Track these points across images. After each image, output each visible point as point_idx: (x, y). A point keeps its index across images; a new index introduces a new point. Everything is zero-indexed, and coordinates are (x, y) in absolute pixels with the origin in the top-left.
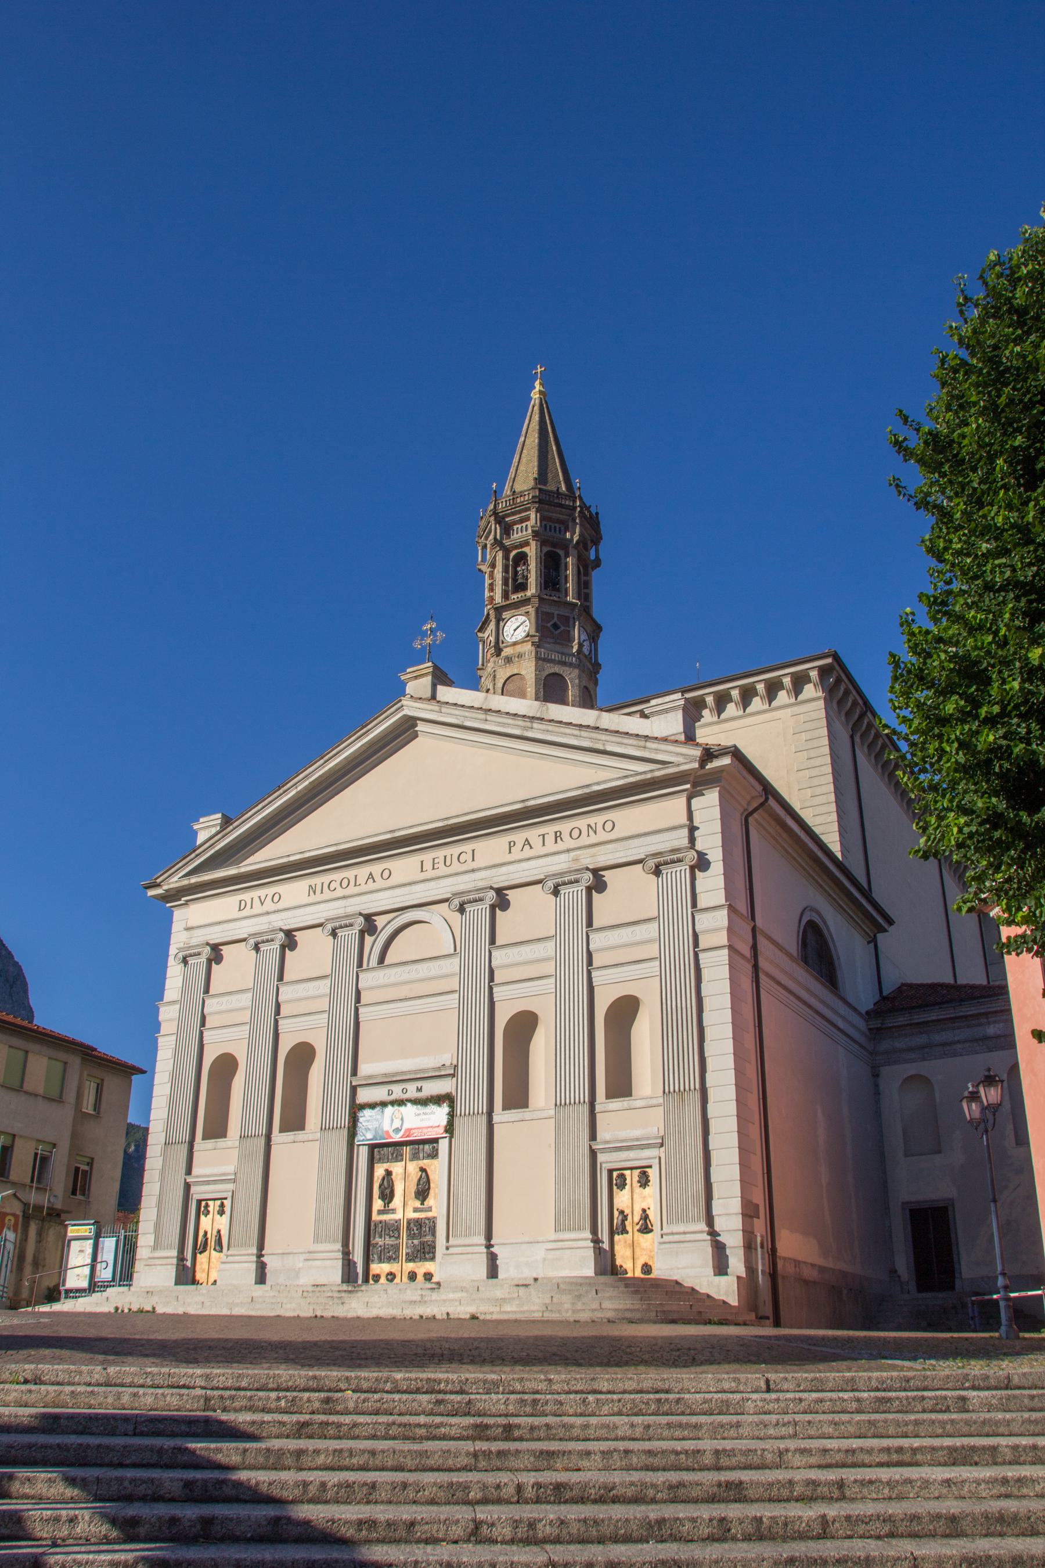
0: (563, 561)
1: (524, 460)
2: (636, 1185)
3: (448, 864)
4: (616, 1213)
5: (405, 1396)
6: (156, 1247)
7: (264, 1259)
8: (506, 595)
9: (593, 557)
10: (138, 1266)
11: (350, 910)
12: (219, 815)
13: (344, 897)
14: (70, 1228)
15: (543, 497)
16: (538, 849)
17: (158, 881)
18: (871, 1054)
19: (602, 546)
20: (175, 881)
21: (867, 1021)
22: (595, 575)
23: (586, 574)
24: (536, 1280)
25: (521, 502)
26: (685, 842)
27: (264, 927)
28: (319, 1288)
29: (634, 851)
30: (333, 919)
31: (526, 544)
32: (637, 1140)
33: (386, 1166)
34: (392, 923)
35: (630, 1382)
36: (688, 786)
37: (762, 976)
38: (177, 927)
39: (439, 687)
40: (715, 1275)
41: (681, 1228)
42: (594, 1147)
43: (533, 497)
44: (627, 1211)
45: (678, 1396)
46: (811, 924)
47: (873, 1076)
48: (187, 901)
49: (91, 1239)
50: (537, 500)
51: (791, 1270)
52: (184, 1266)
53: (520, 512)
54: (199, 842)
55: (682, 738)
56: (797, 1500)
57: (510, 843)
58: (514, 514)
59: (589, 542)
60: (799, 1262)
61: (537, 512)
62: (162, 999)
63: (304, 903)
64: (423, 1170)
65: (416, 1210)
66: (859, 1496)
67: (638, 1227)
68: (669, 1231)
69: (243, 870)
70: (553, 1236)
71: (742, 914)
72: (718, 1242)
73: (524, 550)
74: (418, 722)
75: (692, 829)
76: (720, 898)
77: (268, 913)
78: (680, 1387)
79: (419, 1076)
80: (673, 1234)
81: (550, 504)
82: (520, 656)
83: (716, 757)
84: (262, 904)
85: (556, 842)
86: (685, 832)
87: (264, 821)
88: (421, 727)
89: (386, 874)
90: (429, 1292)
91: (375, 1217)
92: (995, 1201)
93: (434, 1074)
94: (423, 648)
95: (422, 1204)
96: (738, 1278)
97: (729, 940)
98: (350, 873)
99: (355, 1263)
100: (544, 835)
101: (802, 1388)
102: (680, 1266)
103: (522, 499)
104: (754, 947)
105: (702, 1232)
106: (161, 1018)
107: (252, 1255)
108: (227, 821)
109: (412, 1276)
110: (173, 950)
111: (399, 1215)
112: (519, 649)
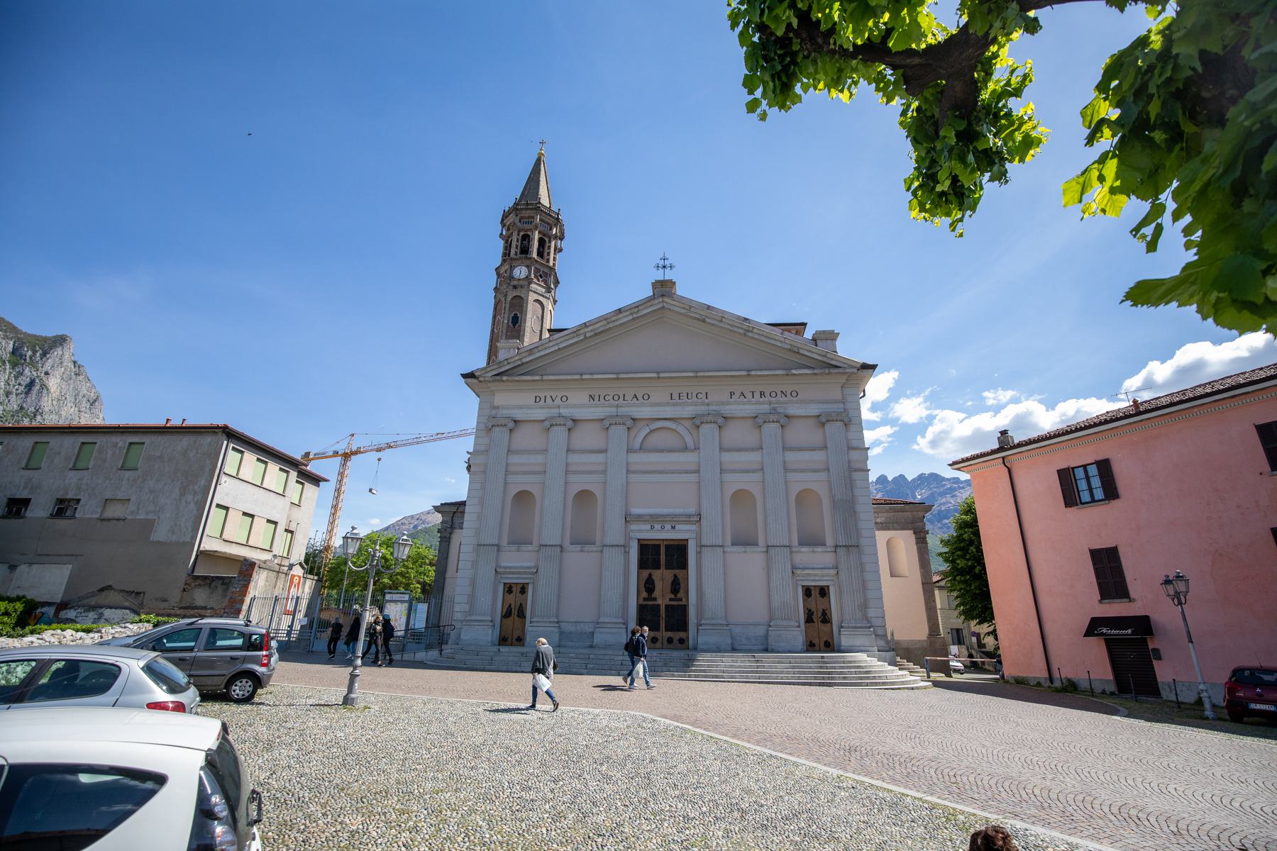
0: (547, 244)
2: (818, 596)
8: (516, 254)
33: (649, 571)
57: (731, 393)
64: (675, 576)
65: (671, 600)
67: (820, 620)
82: (522, 287)
92: (1191, 641)
95: (675, 596)
109: (670, 640)
112: (521, 283)
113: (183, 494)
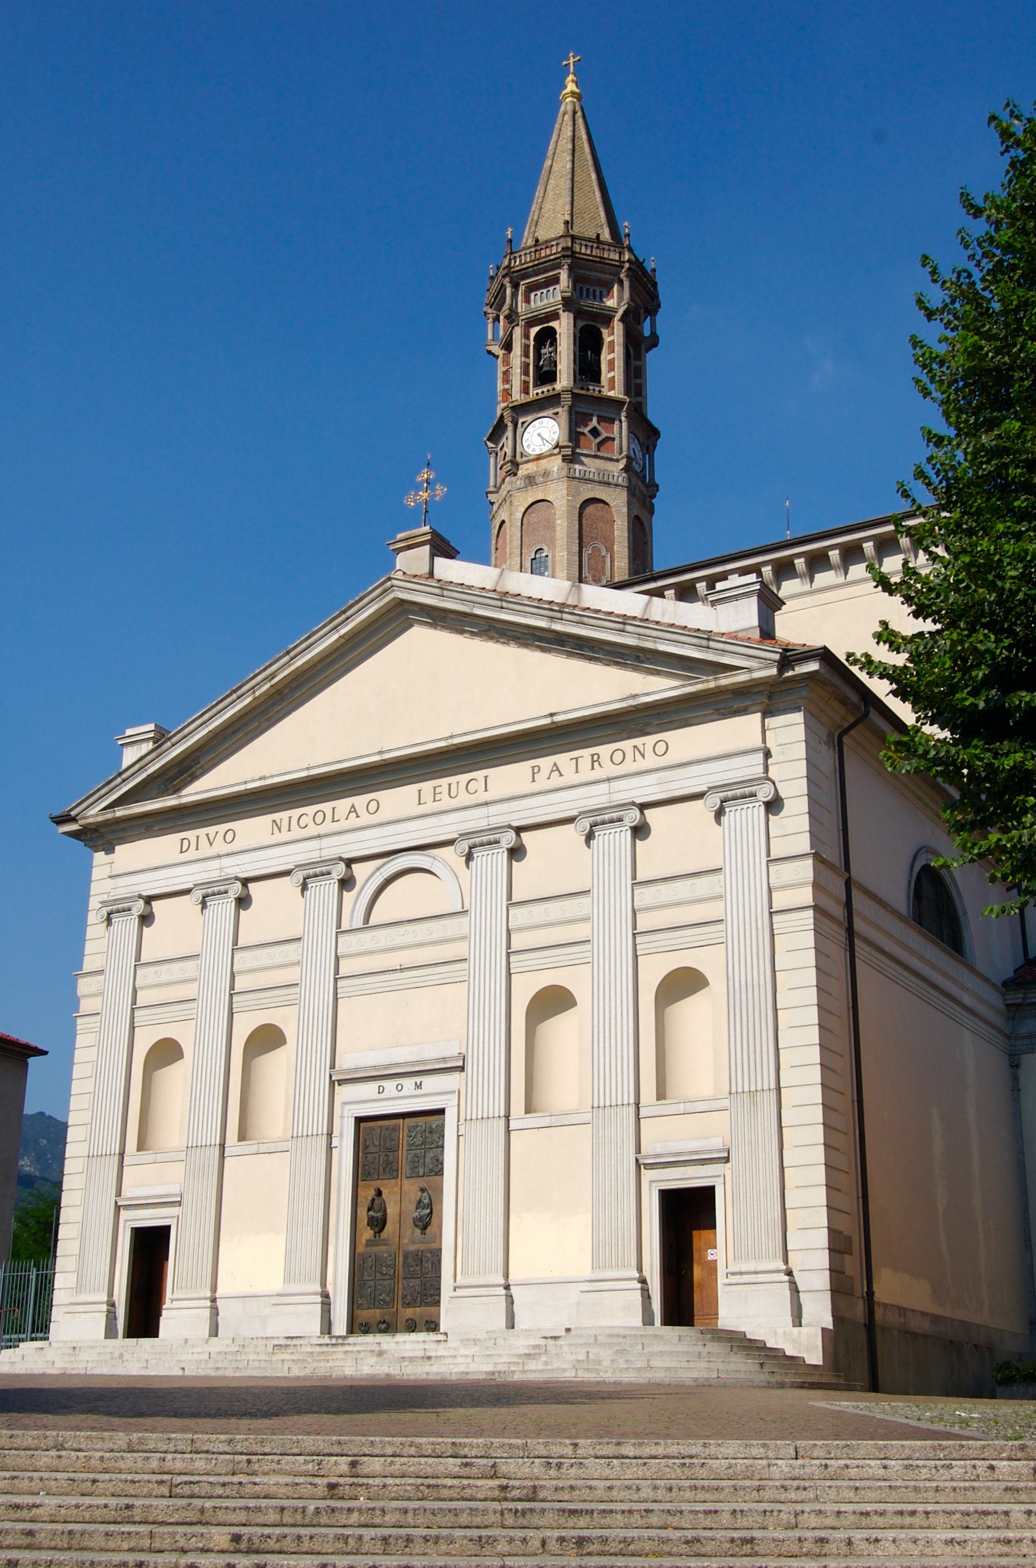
1: (550, 194)
3: (453, 793)
5: (431, 1460)
6: (79, 1288)
8: (526, 390)
9: (647, 333)
10: (56, 1314)
11: (327, 854)
12: (151, 727)
13: (319, 837)
17: (73, 813)
18: (1009, 1038)
19: (659, 318)
21: (1004, 995)
22: (652, 359)
23: (639, 357)
24: (568, 1330)
25: (546, 256)
26: (760, 769)
27: (215, 875)
28: (294, 1342)
29: (694, 781)
30: (305, 865)
31: (554, 316)
32: (696, 1153)
34: (382, 870)
35: (658, 1447)
37: (857, 941)
38: (97, 873)
39: (439, 561)
40: (794, 1326)
41: (752, 1266)
43: (563, 249)
45: (702, 1461)
46: (927, 868)
47: (1012, 1066)
51: (893, 1319)
54: (124, 766)
55: (756, 634)
56: (806, 1555)
59: (642, 311)
60: (905, 1309)
62: (80, 965)
63: (267, 843)
66: (865, 1553)
68: (737, 1270)
69: (185, 800)
73: (551, 324)
75: (767, 754)
76: (803, 843)
77: (219, 856)
78: (707, 1453)
80: (741, 1273)
82: (546, 474)
84: (211, 844)
85: (593, 768)
86: (760, 757)
87: (211, 735)
89: (373, 806)
90: (434, 1346)
93: (437, 1066)
94: (418, 505)
96: (824, 1330)
97: (814, 900)
100: (577, 759)
101: (832, 1455)
103: (548, 253)
104: (848, 905)
105: (778, 1271)
106: (79, 993)
107: (206, 1298)
108: (161, 737)
110: (94, 903)
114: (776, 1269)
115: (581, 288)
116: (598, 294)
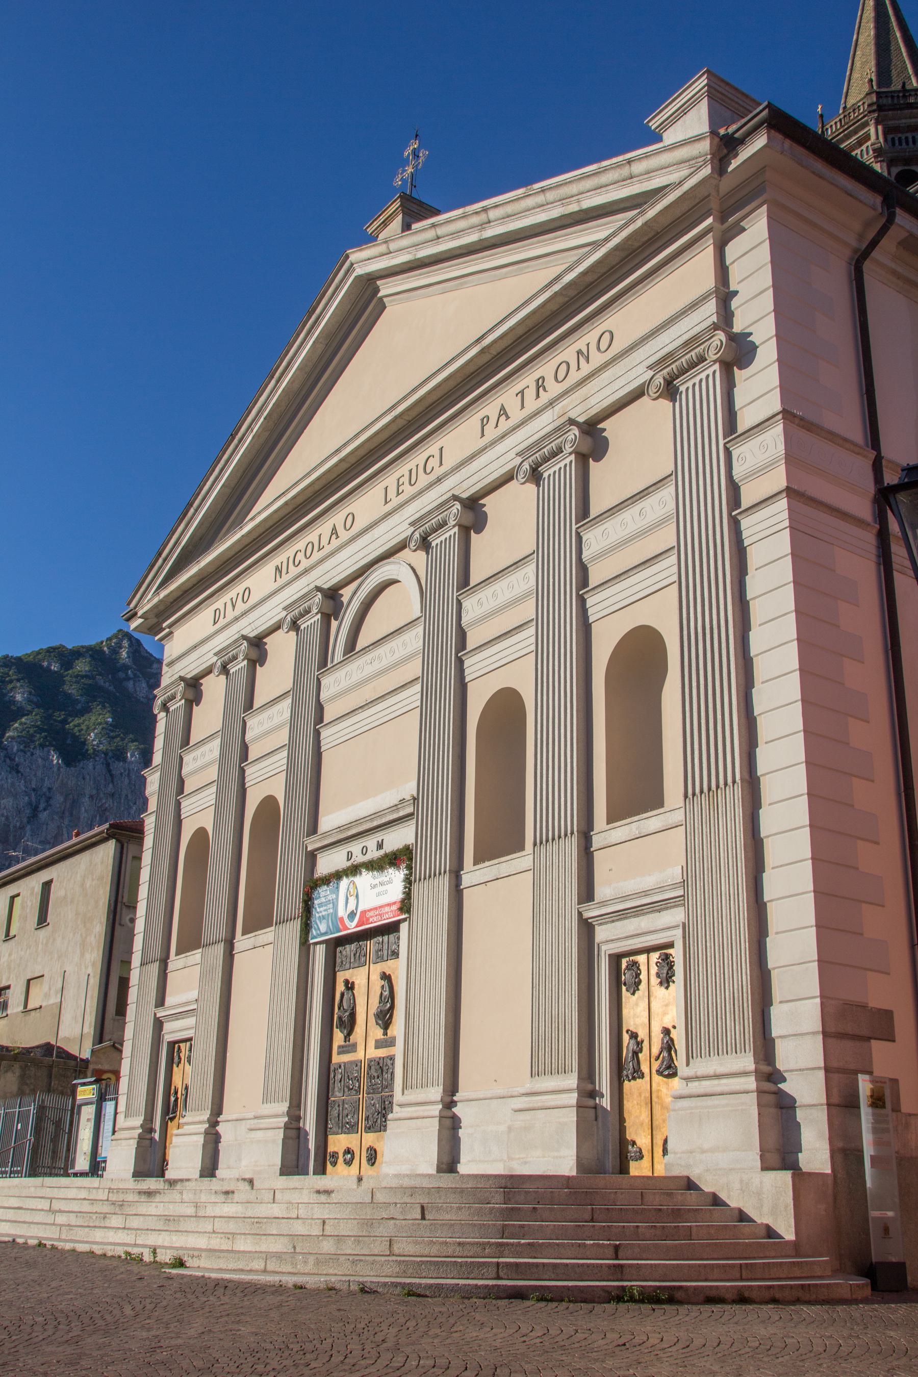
2: (654, 981)
4: (626, 1037)
7: (220, 1128)
14: (80, 1089)
15: (884, 101)
16: (517, 415)
17: (132, 606)
20: (149, 602)
25: (854, 118)
36: (710, 220)
40: (765, 1168)
42: (586, 915)
43: (869, 105)
44: (642, 1034)
48: (170, 626)
49: (91, 1103)
50: (875, 107)
52: (152, 1139)
53: (855, 132)
58: (848, 137)
61: (877, 123)
70: (530, 1085)
71: (856, 445)
72: (780, 1093)
74: (379, 283)
79: (375, 823)
81: (894, 108)
83: (742, 141)
88: (386, 288)
91: (336, 1059)
98: (312, 536)
99: (307, 1134)
102: (706, 1146)
105: (745, 1074)
111: (360, 1055)
113: (82, 954)
114: (742, 1069)
115: (893, 139)
116: (910, 140)
